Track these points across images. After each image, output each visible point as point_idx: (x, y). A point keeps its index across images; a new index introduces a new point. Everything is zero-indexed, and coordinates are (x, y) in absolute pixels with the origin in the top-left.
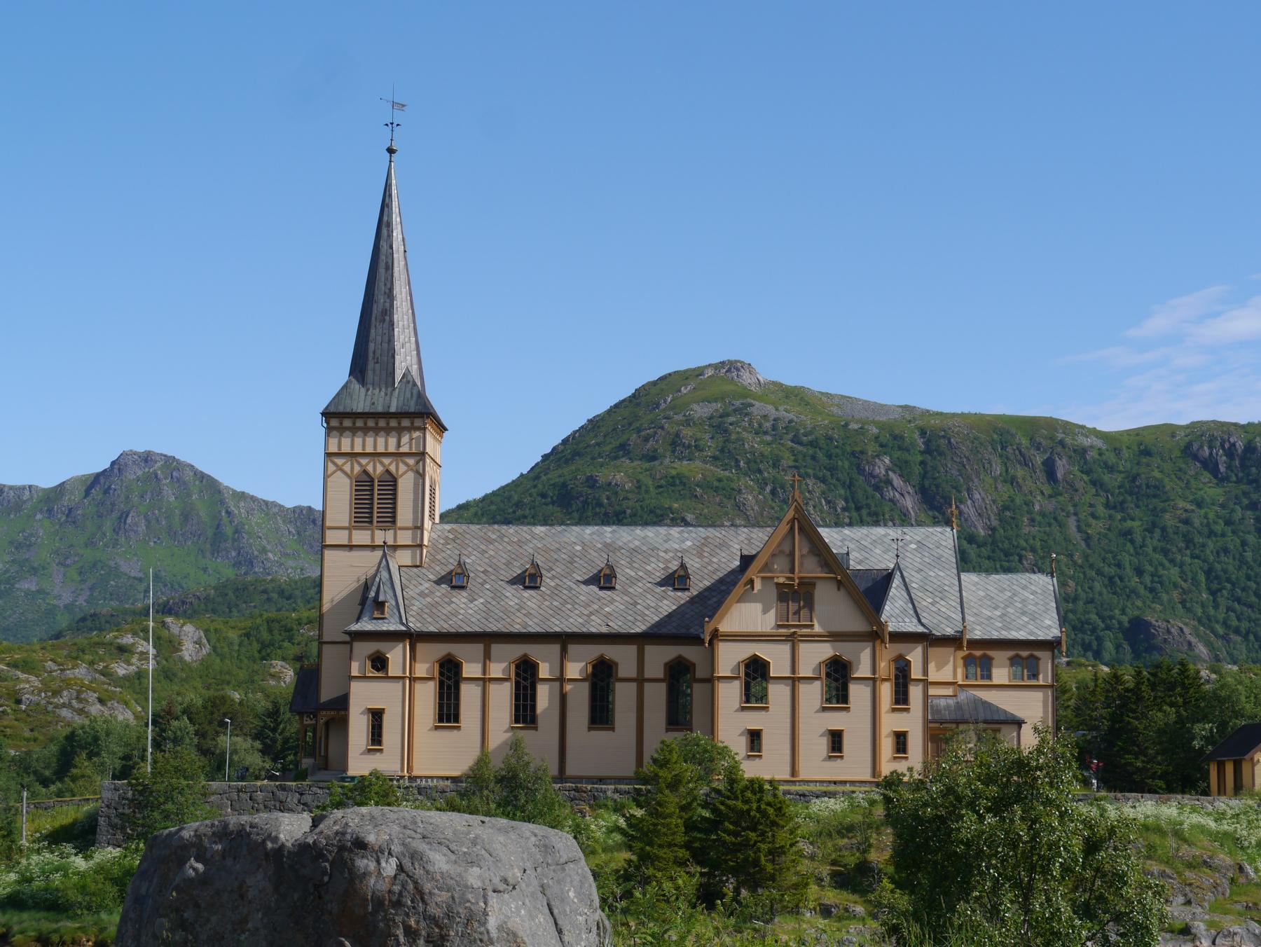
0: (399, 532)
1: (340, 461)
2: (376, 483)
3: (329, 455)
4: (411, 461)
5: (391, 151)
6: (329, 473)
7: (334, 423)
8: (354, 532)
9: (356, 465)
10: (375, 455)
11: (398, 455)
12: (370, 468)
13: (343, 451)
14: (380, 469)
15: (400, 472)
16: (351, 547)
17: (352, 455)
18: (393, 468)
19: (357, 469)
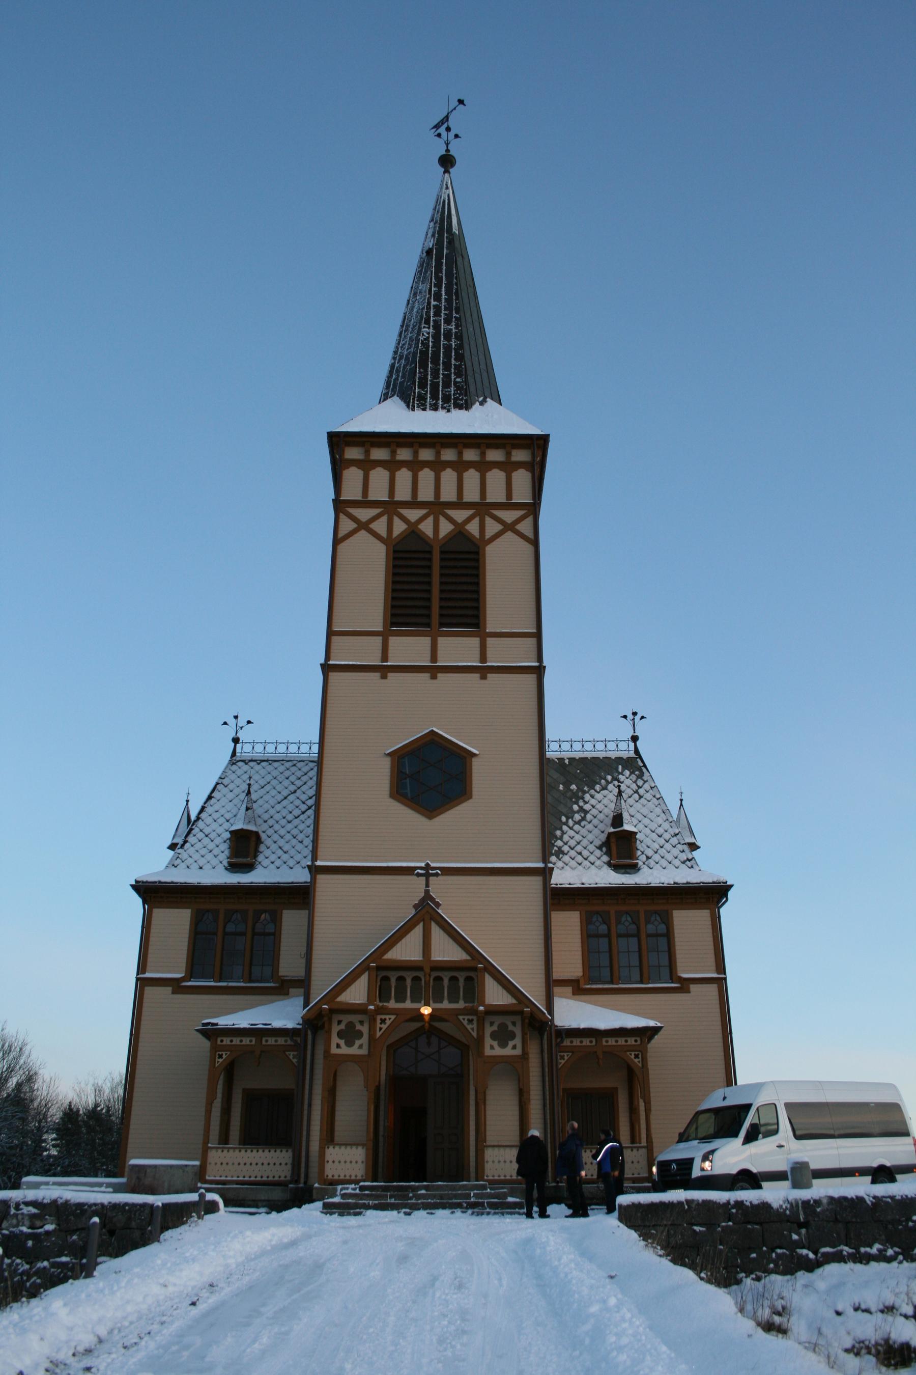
0: (490, 641)
1: (363, 514)
2: (436, 557)
3: (340, 506)
4: (509, 516)
5: (447, 161)
6: (341, 535)
7: (353, 453)
8: (393, 641)
9: (396, 520)
10: (437, 507)
11: (483, 508)
12: (427, 528)
13: (372, 497)
14: (446, 528)
15: (489, 533)
16: (384, 671)
17: (391, 507)
18: (473, 528)
19: (399, 527)
